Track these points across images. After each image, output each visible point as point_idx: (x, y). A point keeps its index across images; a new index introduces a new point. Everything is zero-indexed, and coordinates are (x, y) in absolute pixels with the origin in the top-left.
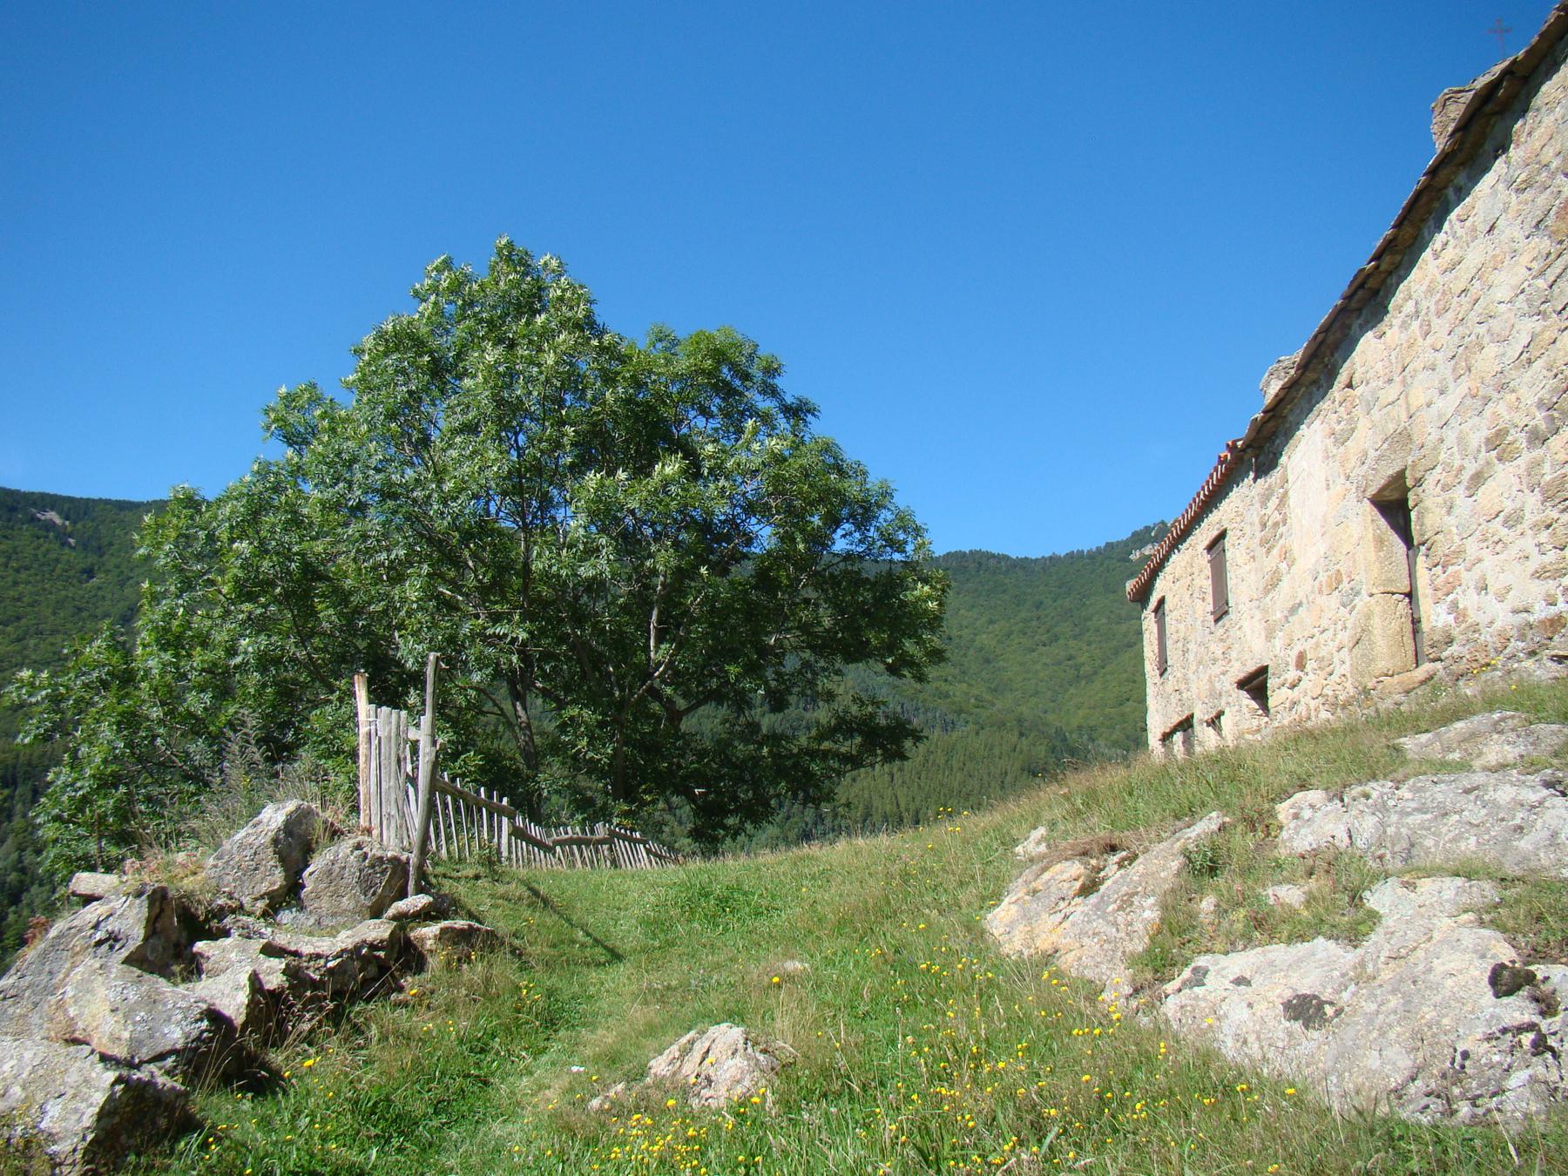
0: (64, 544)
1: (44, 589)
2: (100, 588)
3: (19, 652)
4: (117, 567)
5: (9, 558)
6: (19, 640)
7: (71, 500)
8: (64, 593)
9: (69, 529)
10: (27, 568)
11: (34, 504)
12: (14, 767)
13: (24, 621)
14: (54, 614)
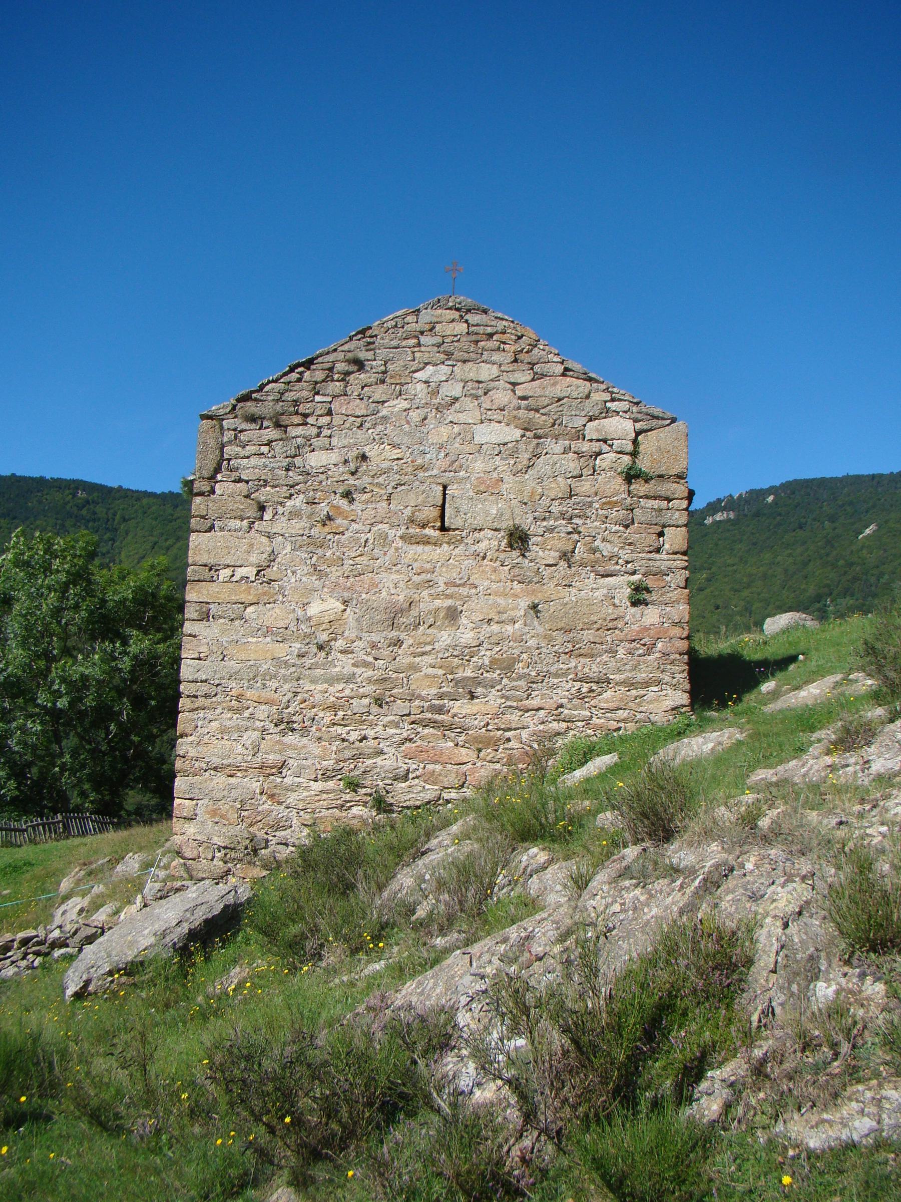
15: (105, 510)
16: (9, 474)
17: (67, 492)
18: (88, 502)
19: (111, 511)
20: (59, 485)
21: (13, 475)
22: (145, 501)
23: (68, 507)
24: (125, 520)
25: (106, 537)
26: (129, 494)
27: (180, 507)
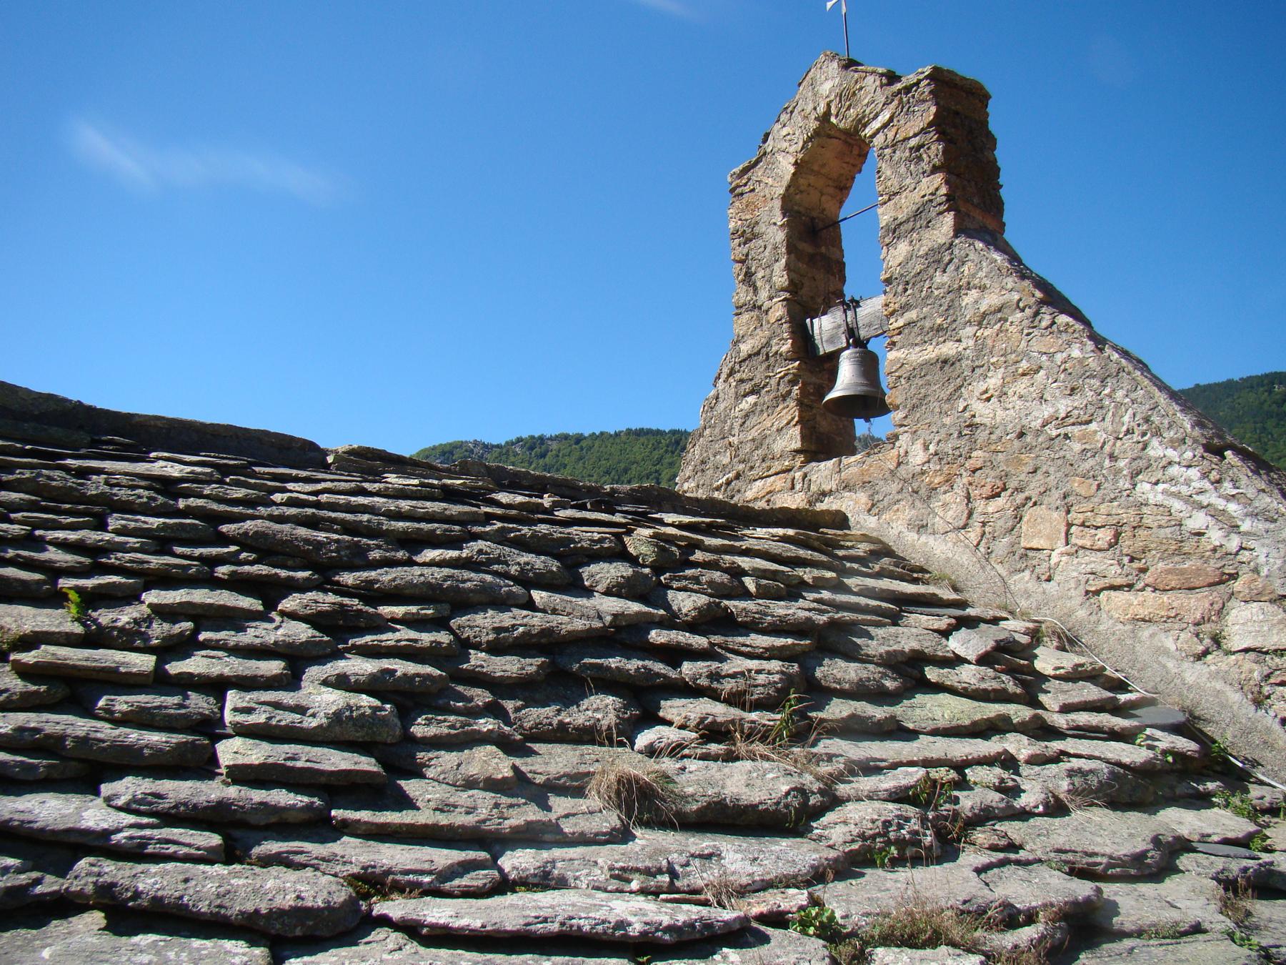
16: (1191, 386)
21: (1197, 386)
23: (1266, 407)
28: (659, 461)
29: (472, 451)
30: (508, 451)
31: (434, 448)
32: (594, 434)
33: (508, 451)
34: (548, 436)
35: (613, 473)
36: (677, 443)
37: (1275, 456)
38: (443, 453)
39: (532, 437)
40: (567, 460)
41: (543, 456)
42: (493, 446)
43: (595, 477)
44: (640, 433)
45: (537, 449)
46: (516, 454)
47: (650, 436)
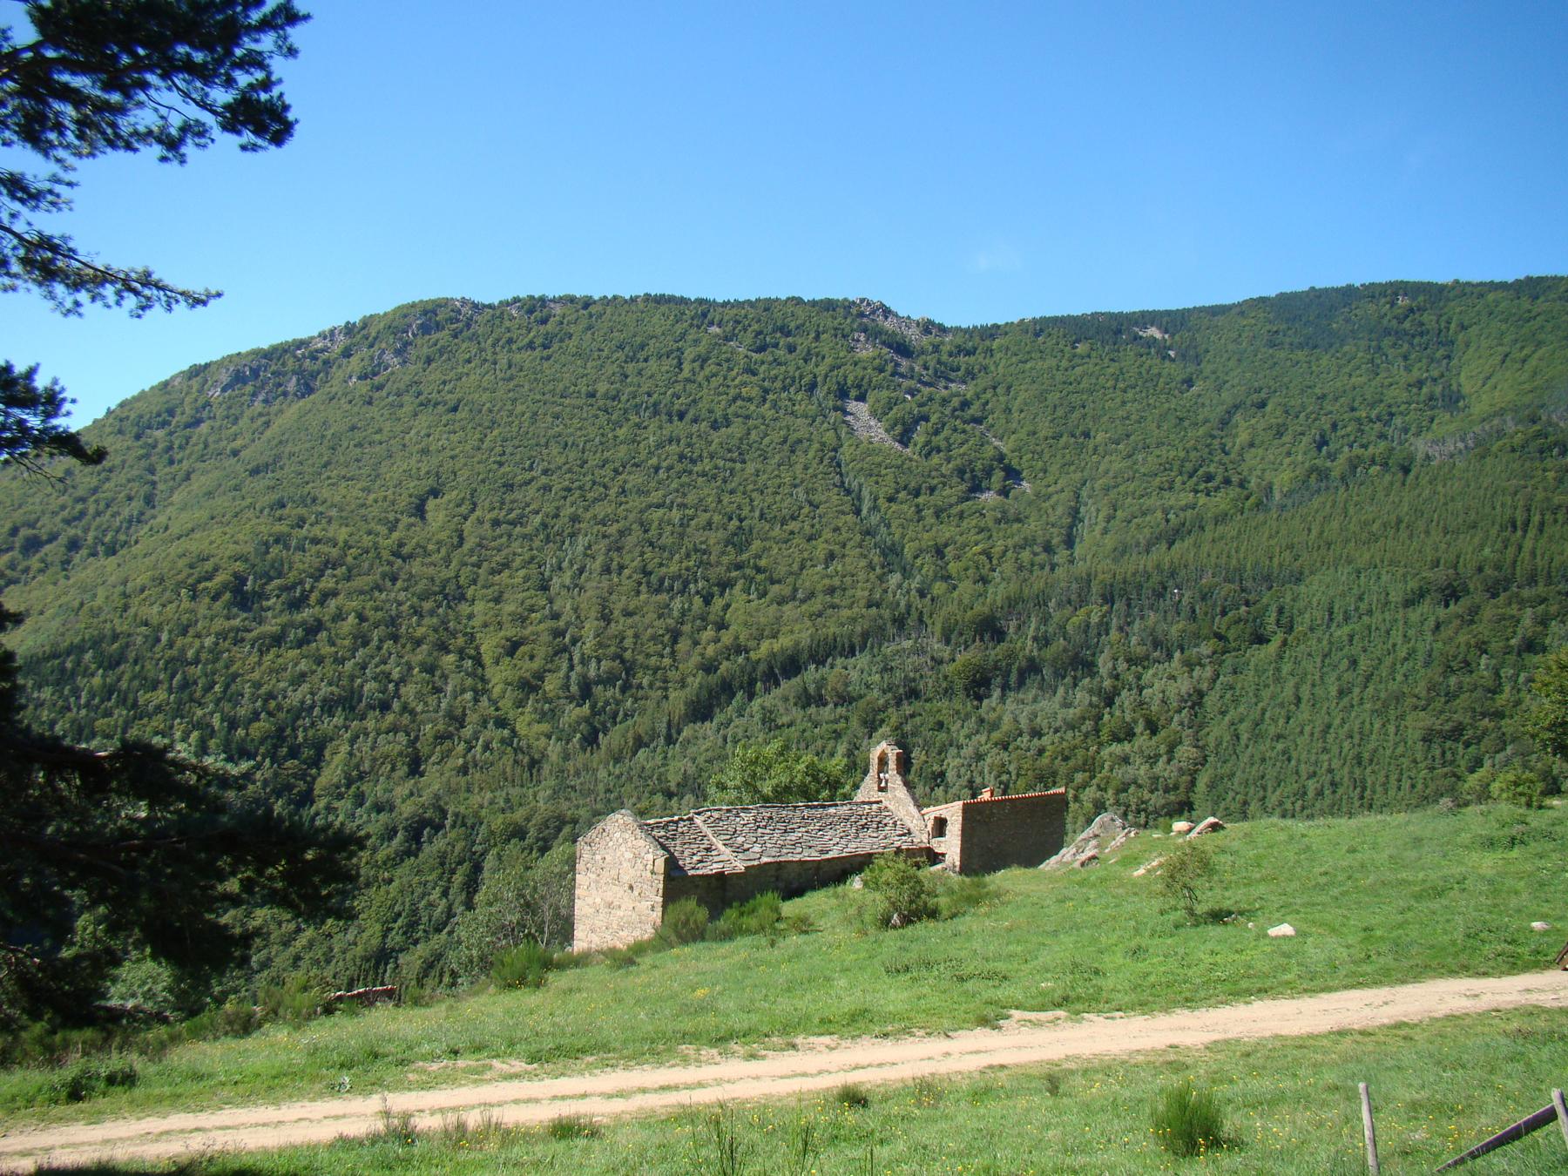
0: (1166, 357)
1: (1149, 405)
2: (1199, 395)
3: (1130, 468)
4: (1214, 372)
5: (1117, 380)
6: (1130, 456)
7: (1168, 313)
8: (1166, 405)
9: (1168, 343)
10: (1133, 387)
11: (1136, 324)
12: (1112, 586)
13: (1132, 438)
14: (1159, 427)
15: (1435, 318)
16: (1305, 288)
17: (1383, 300)
18: (1411, 310)
19: (1444, 318)
20: (1373, 292)
21: (1313, 289)
22: (1491, 297)
23: (1385, 322)
24: (1463, 327)
25: (1438, 355)
26: (1468, 290)
27: (1542, 299)
28: (683, 336)
29: (459, 312)
30: (502, 313)
31: (413, 305)
32: (605, 297)
33: (502, 313)
34: (551, 296)
35: (627, 349)
36: (704, 315)
37: (1386, 382)
38: (425, 313)
39: (531, 298)
40: (572, 328)
41: (544, 321)
42: (485, 306)
43: (606, 352)
44: (661, 300)
45: (537, 314)
46: (512, 318)
47: (672, 305)
